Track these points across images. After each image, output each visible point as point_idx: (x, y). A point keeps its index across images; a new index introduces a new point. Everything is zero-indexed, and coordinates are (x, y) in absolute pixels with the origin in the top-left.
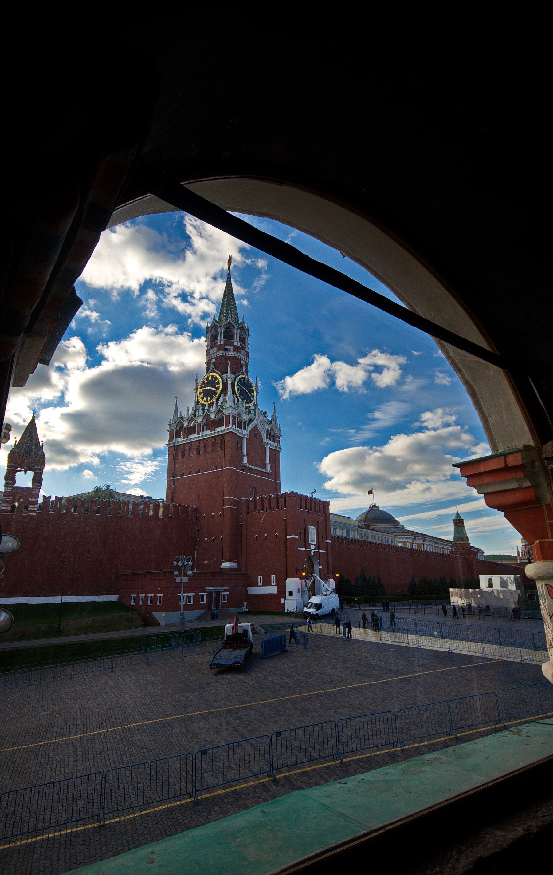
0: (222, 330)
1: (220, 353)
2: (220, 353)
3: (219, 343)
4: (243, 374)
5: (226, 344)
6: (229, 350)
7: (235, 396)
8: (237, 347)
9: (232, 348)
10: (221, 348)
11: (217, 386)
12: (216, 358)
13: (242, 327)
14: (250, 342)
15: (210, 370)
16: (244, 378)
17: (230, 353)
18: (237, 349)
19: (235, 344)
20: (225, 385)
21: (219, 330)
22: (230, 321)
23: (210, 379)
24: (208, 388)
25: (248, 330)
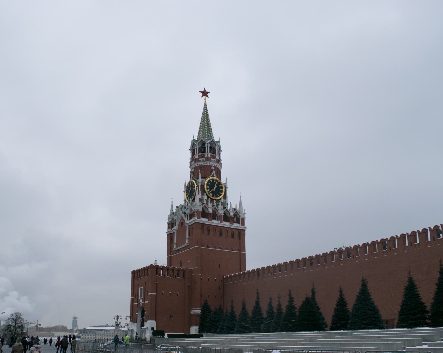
2: (196, 164)
4: (213, 176)
5: (200, 157)
6: (202, 161)
7: (205, 194)
8: (208, 157)
9: (204, 159)
12: (195, 168)
13: (213, 141)
16: (213, 180)
17: (203, 163)
18: (208, 159)
19: (206, 156)
22: (202, 140)
25: (219, 142)
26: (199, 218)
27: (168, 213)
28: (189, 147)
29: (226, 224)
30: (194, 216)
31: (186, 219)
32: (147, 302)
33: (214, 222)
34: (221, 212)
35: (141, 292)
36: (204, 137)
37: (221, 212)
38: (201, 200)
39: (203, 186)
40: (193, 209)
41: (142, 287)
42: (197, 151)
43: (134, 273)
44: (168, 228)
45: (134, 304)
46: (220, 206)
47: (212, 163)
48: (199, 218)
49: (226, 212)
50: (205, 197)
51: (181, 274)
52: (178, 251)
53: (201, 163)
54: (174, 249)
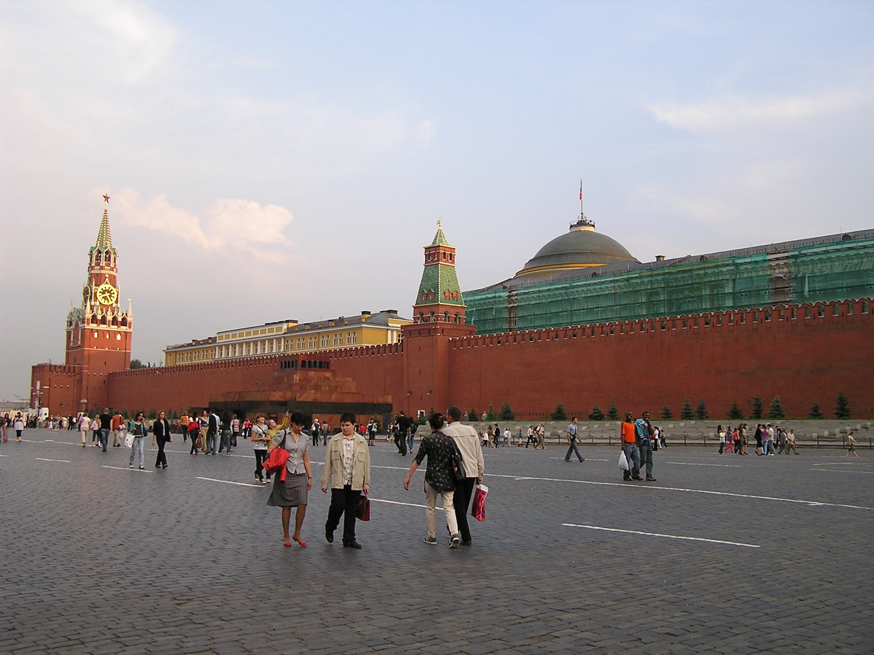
5: (98, 264)
18: (102, 268)
26: (88, 324)
27: (67, 314)
28: (89, 252)
29: (114, 328)
33: (103, 327)
34: (109, 318)
36: (101, 245)
37: (109, 318)
38: (92, 308)
39: (96, 293)
43: (33, 367)
46: (109, 312)
47: (106, 272)
48: (88, 324)
49: (115, 319)
50: (98, 304)
51: (72, 371)
52: (73, 348)
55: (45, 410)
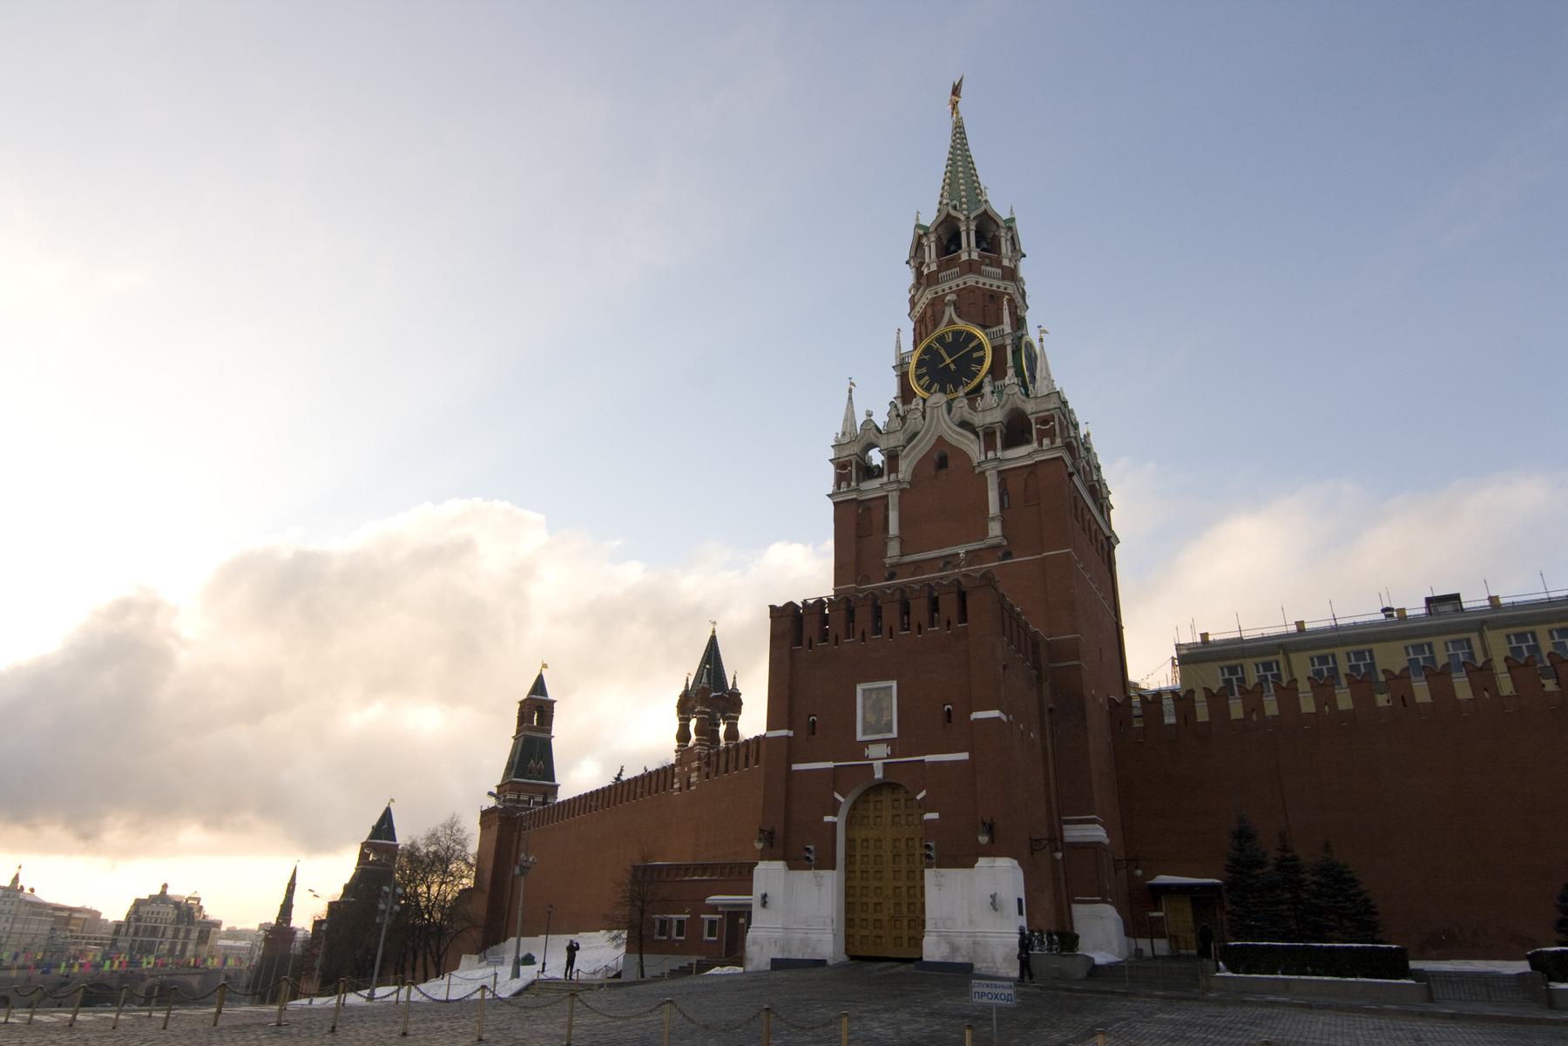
0: (973, 227)
1: (971, 280)
2: (971, 280)
3: (964, 257)
6: (988, 276)
10: (971, 267)
11: (975, 355)
12: (959, 293)
14: (1025, 269)
15: (946, 320)
17: (996, 283)
19: (1006, 262)
20: (998, 351)
21: (963, 228)
22: (985, 212)
23: (950, 339)
24: (948, 361)
30: (1050, 434)
31: (973, 448)
32: (964, 756)
35: (878, 707)
40: (1029, 407)
41: (894, 684)
42: (968, 239)
44: (840, 479)
45: (795, 767)
53: (988, 281)
54: (888, 561)
55: (1001, 877)
